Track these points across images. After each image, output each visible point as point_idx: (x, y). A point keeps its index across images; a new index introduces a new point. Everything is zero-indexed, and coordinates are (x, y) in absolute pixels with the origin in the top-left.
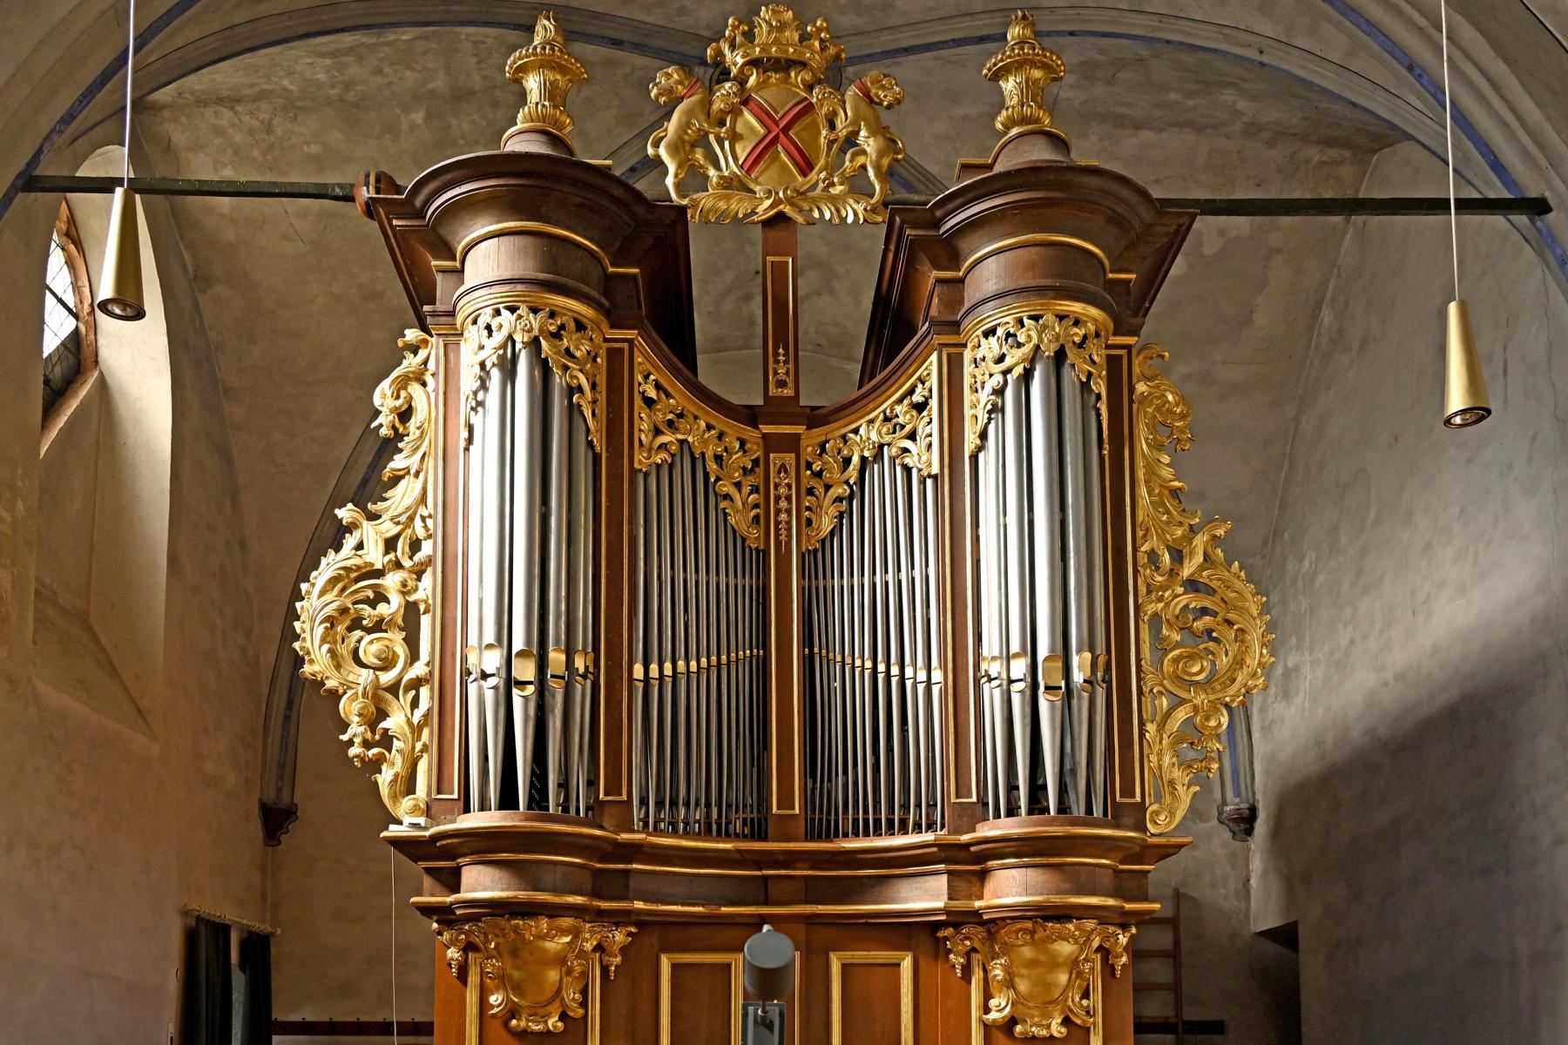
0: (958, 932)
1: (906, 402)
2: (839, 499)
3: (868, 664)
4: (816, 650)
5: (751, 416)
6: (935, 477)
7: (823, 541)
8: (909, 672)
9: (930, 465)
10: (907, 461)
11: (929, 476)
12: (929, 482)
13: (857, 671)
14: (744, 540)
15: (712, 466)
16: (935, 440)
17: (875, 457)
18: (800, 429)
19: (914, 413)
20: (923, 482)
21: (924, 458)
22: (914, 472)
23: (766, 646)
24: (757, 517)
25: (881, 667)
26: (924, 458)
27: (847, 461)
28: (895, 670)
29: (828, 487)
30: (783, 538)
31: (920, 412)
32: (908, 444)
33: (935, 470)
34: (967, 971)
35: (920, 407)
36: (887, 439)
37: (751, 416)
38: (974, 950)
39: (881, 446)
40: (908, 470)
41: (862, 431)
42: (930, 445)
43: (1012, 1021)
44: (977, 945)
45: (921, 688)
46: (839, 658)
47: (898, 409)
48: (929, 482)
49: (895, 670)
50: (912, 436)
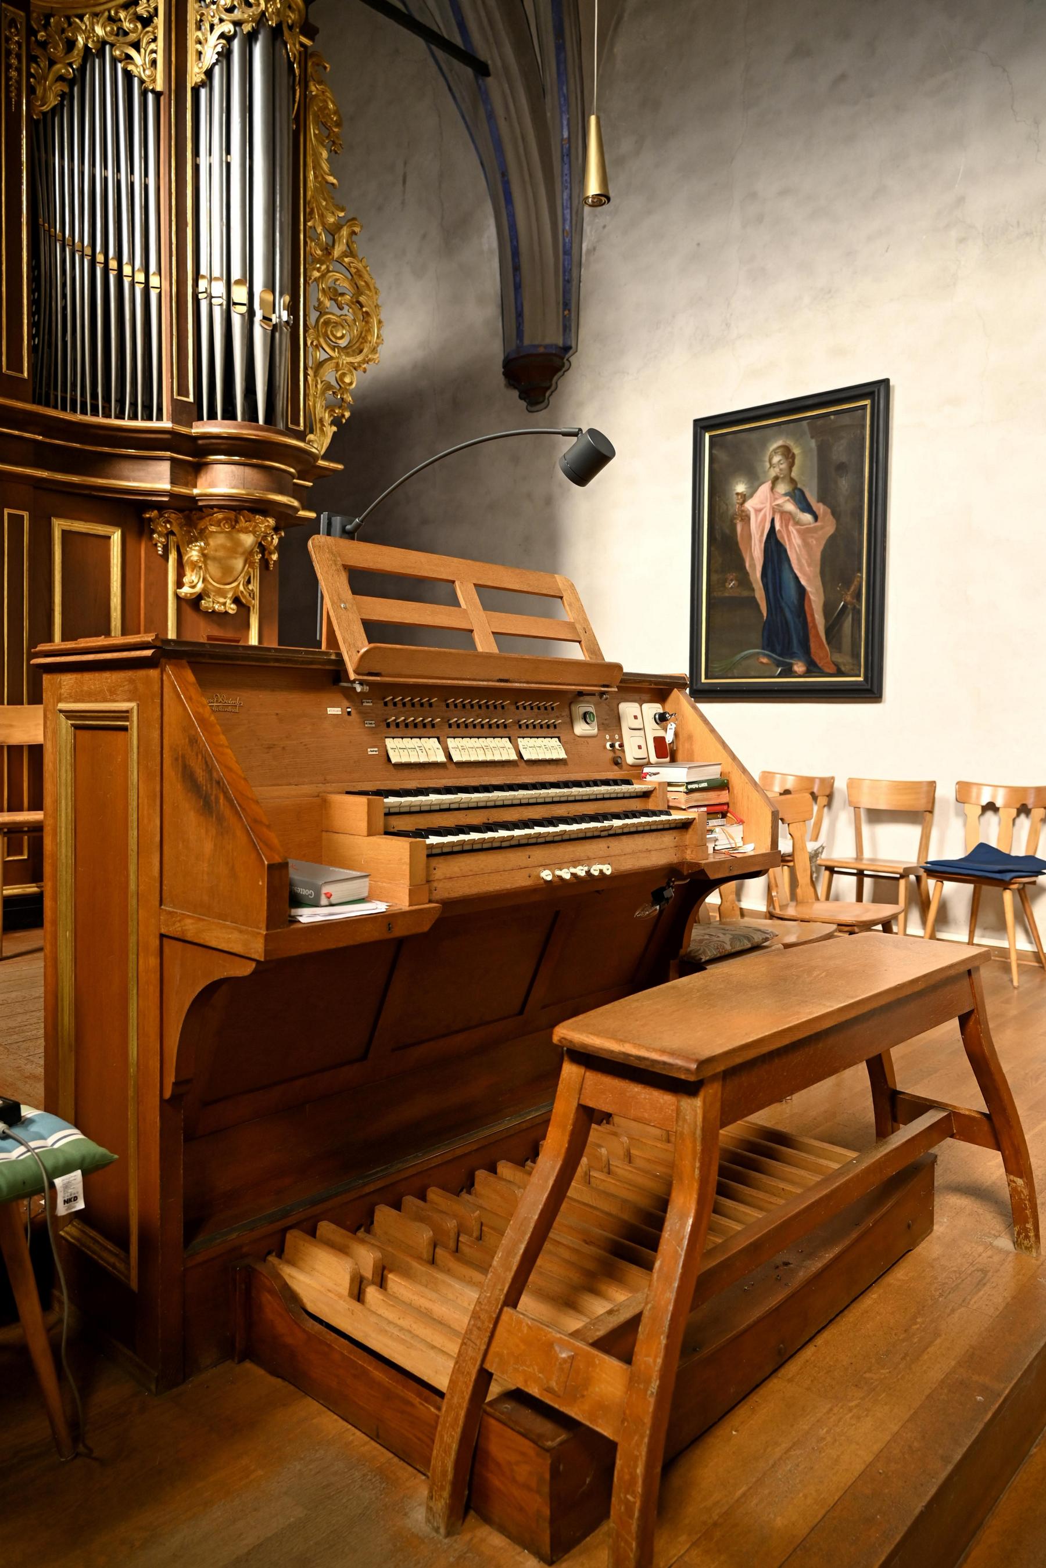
0: (161, 516)
1: (131, 11)
2: (61, 78)
7: (45, 114)
9: (154, 81)
10: (130, 68)
11: (153, 91)
16: (160, 58)
17: (98, 51)
19: (139, 26)
21: (148, 72)
22: (136, 81)
26: (148, 72)
27: (71, 44)
29: (52, 63)
31: (144, 26)
32: (133, 52)
34: (166, 549)
35: (146, 22)
36: (111, 39)
38: (172, 533)
39: (104, 43)
40: (128, 76)
42: (154, 62)
43: (200, 597)
44: (176, 530)
47: (122, 15)
50: (136, 46)
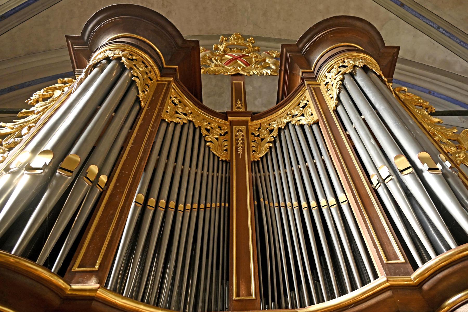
3: (295, 204)
4: (262, 199)
5: (224, 116)
6: (317, 123)
8: (323, 202)
12: (314, 127)
13: (289, 209)
14: (219, 158)
15: (204, 132)
18: (249, 119)
20: (311, 127)
23: (230, 201)
24: (226, 150)
25: (304, 204)
28: (313, 204)
30: (240, 152)
33: (316, 117)
37: (224, 116)
40: (302, 126)
41: (277, 120)
45: (333, 209)
46: (276, 204)
48: (314, 127)
49: (313, 204)
